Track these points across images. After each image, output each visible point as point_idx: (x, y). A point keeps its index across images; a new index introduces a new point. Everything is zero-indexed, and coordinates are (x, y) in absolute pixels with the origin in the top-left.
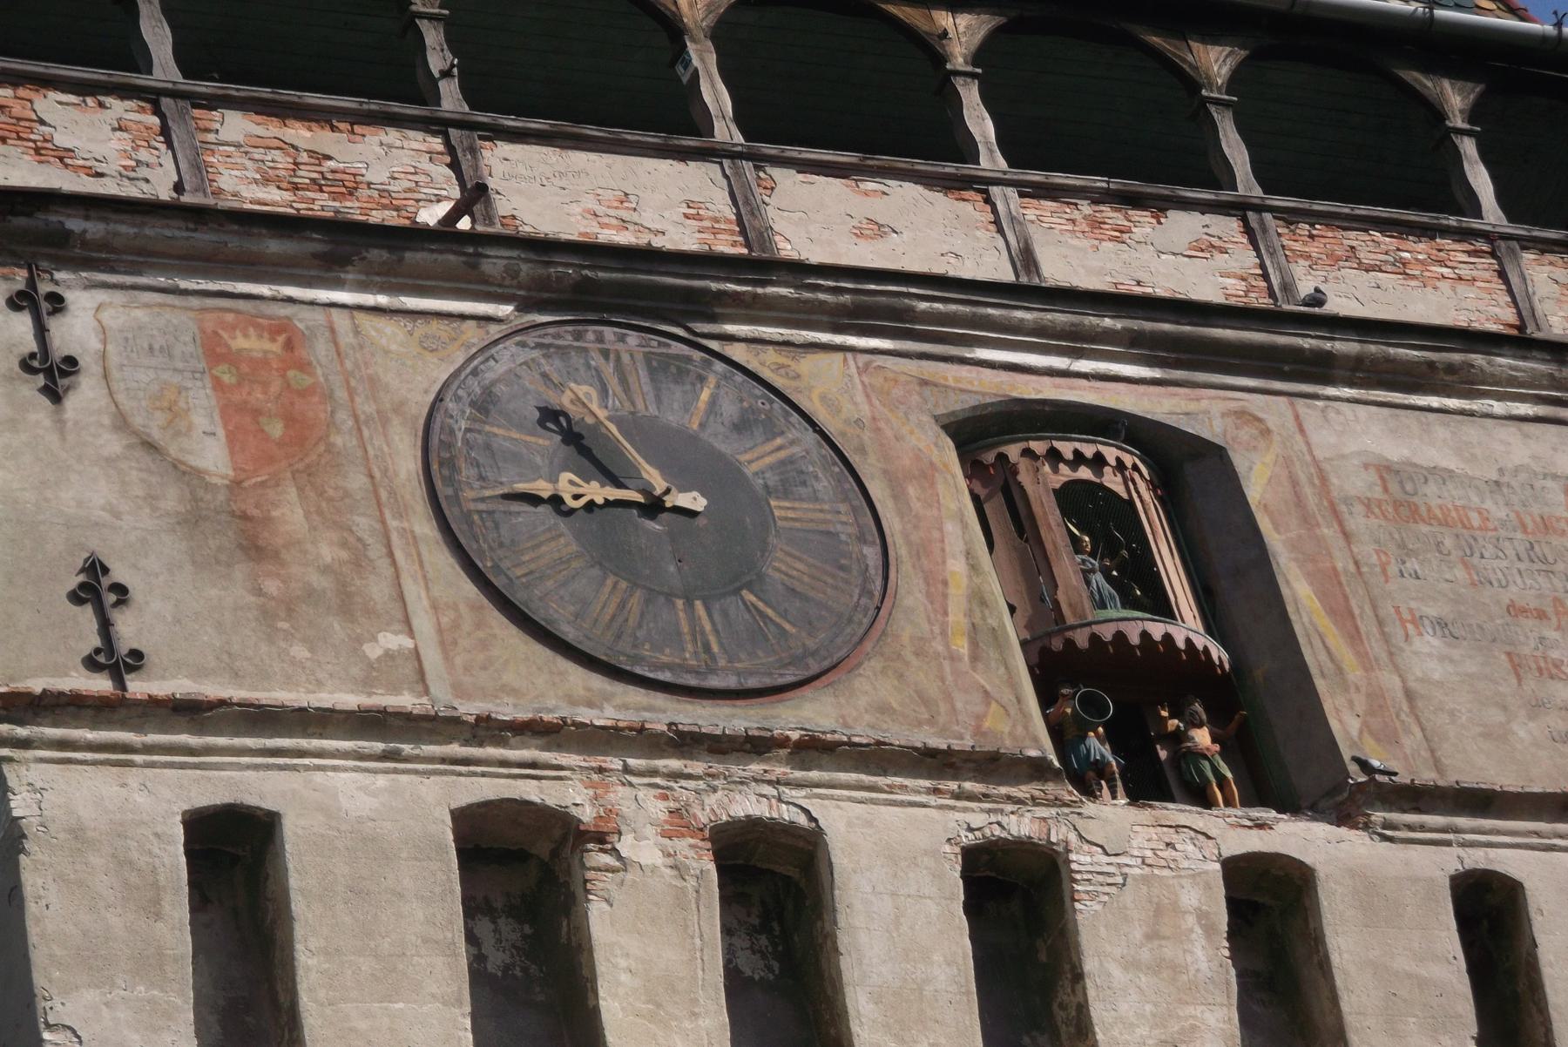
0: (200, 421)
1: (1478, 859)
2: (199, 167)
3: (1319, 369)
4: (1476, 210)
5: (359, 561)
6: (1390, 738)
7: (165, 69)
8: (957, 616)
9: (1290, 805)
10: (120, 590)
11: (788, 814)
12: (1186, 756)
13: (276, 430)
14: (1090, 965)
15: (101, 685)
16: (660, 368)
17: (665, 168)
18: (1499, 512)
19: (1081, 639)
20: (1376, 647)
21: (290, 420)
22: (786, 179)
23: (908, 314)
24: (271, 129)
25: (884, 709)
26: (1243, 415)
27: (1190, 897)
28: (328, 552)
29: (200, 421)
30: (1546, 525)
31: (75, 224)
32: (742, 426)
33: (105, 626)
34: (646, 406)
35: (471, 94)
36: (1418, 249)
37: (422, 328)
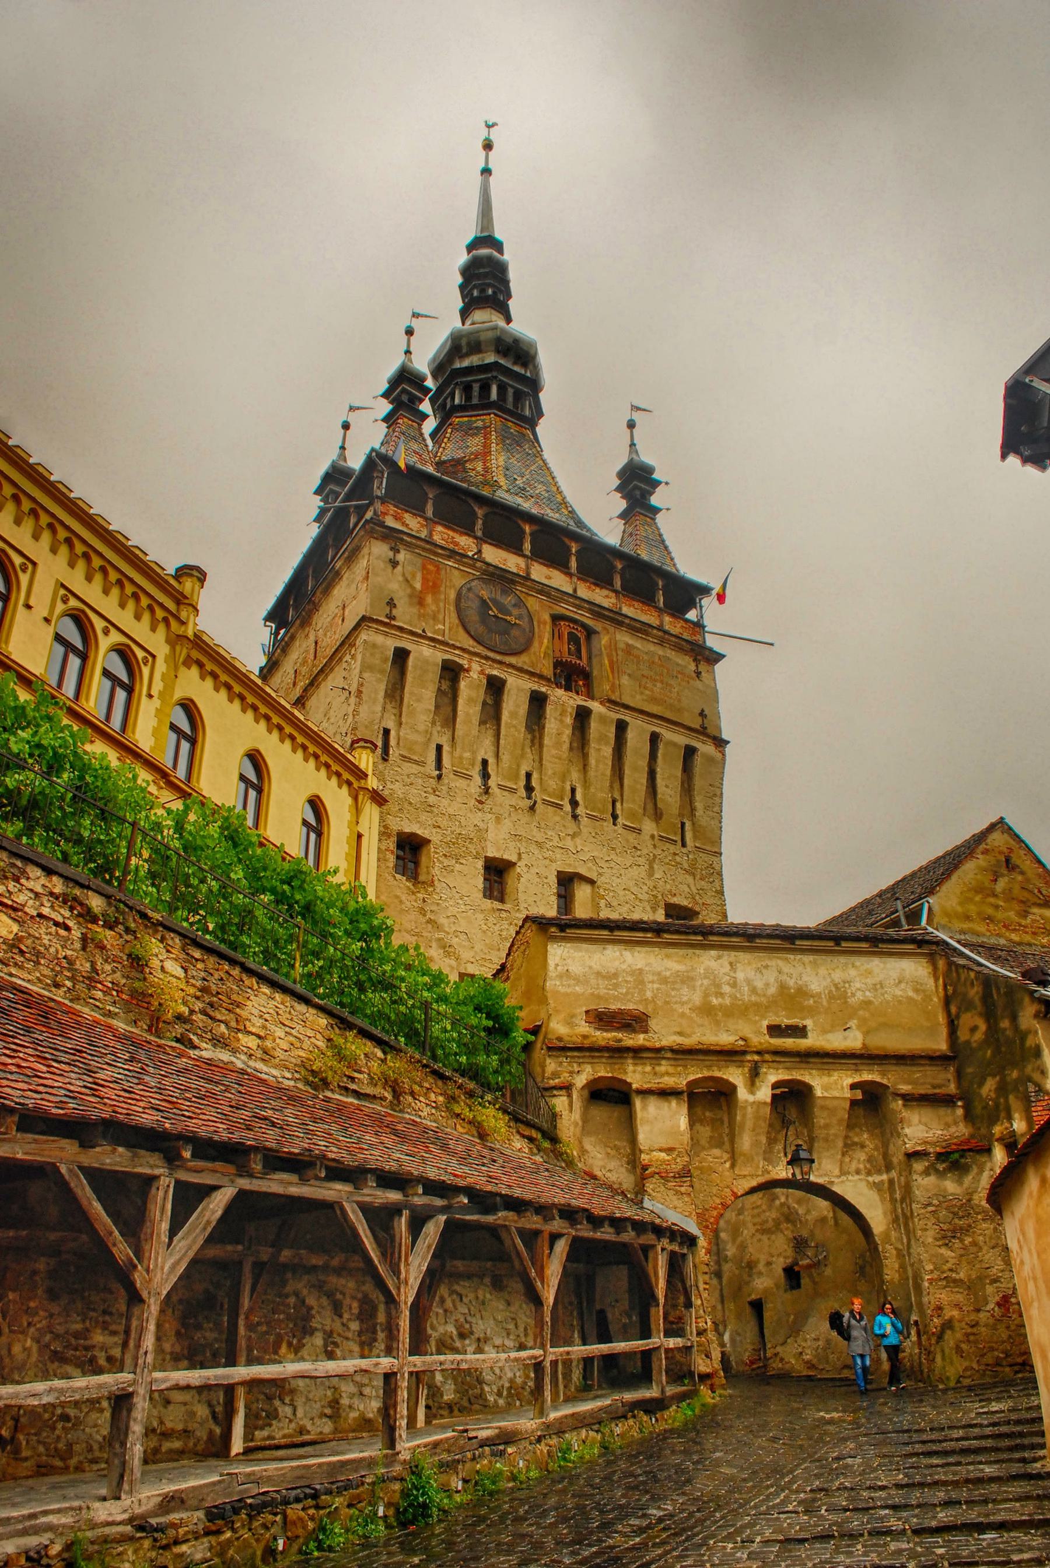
1: (622, 717)
2: (431, 535)
3: (620, 624)
5: (439, 611)
6: (613, 692)
7: (430, 513)
8: (543, 650)
9: (593, 698)
18: (646, 658)
22: (535, 564)
27: (569, 710)
28: (434, 608)
30: (653, 662)
32: (515, 605)
34: (498, 597)
35: (483, 533)
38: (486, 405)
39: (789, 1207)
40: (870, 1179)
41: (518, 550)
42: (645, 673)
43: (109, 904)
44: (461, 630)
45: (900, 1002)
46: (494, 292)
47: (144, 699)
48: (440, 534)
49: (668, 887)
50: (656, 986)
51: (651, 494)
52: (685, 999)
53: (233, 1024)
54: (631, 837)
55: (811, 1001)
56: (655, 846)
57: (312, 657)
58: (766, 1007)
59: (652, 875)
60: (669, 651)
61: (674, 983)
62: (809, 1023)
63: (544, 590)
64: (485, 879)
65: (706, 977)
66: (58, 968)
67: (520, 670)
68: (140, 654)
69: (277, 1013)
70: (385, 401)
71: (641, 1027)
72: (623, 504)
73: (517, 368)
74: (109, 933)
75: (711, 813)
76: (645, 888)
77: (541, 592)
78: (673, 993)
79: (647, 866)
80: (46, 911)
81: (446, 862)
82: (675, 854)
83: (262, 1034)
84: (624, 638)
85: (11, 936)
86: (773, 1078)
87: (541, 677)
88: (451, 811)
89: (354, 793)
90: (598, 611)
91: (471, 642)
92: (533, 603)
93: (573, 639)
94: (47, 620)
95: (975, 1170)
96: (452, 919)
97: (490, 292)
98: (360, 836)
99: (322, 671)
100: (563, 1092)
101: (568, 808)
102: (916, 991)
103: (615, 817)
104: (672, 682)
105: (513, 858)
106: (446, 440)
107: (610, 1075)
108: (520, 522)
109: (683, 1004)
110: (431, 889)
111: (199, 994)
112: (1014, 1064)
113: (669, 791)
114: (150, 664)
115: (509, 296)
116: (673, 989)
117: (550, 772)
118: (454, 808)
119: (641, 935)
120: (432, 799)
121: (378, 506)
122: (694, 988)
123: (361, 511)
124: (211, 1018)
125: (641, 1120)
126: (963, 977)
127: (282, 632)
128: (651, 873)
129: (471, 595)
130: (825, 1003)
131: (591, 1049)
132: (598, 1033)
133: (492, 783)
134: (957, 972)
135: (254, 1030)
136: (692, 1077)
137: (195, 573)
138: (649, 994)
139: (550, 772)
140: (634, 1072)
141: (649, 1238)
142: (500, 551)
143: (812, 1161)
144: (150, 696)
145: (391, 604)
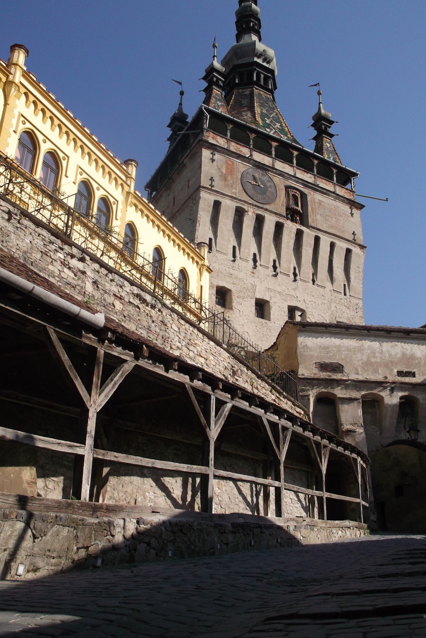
0: (224, 168)
1: (317, 234)
2: (229, 146)
3: (317, 190)
4: (334, 181)
5: (234, 183)
6: (313, 223)
7: (229, 137)
9: (304, 226)
10: (214, 180)
11: (263, 214)
12: (296, 219)
13: (230, 170)
14: (283, 234)
15: (210, 187)
16: (262, 174)
17: (268, 157)
18: (328, 206)
19: (291, 207)
20: (314, 214)
21: (231, 170)
22: (277, 161)
23: (284, 176)
24: (236, 145)
25: (273, 208)
26: (309, 192)
27: (293, 231)
29: (224, 168)
30: (331, 209)
31: (218, 148)
32: (268, 181)
33: (212, 183)
34: (261, 177)
36: (328, 183)
37: (244, 165)
38: (250, 83)
41: (269, 154)
42: (328, 214)
43: (152, 299)
44: (243, 191)
46: (253, 25)
47: (114, 220)
48: (234, 147)
49: (338, 314)
50: (346, 352)
51: (330, 127)
52: (360, 358)
53: (196, 352)
54: (321, 290)
55: (417, 361)
56: (332, 295)
57: (172, 204)
59: (331, 308)
60: (339, 203)
63: (282, 174)
64: (256, 308)
65: (369, 349)
66: (137, 324)
67: (271, 212)
68: (112, 200)
69: (211, 350)
70: (204, 81)
71: (340, 371)
72: (315, 133)
73: (265, 64)
74: (153, 311)
75: (358, 280)
76: (328, 314)
77: (279, 175)
78: (354, 356)
79: (328, 304)
80: (131, 300)
81: (239, 300)
82: (341, 299)
83: (206, 357)
84: (318, 196)
85: (121, 310)
86: (401, 394)
87: (280, 215)
88: (240, 277)
89: (199, 266)
90: (306, 184)
91: (249, 198)
92: (277, 179)
93: (295, 197)
94: (74, 183)
96: (241, 326)
97: (251, 25)
98: (201, 287)
99: (178, 211)
101: (292, 276)
103: (314, 281)
104: (340, 218)
105: (268, 299)
106: (232, 101)
108: (270, 141)
109: (358, 361)
110: (231, 312)
111: (184, 339)
113: (339, 270)
114: (116, 205)
115: (260, 27)
116: (354, 354)
117: (284, 260)
118: (241, 275)
120: (231, 271)
121: (206, 134)
122: (363, 354)
123: (196, 135)
124: (188, 349)
127: (154, 193)
128: (329, 308)
129: (248, 176)
131: (318, 379)
132: (321, 373)
133: (258, 264)
135: (203, 356)
136: (363, 393)
137: (133, 163)
138: (343, 356)
139: (284, 260)
141: (354, 456)
142: (261, 155)
143: (419, 431)
144: (117, 219)
145: (212, 179)
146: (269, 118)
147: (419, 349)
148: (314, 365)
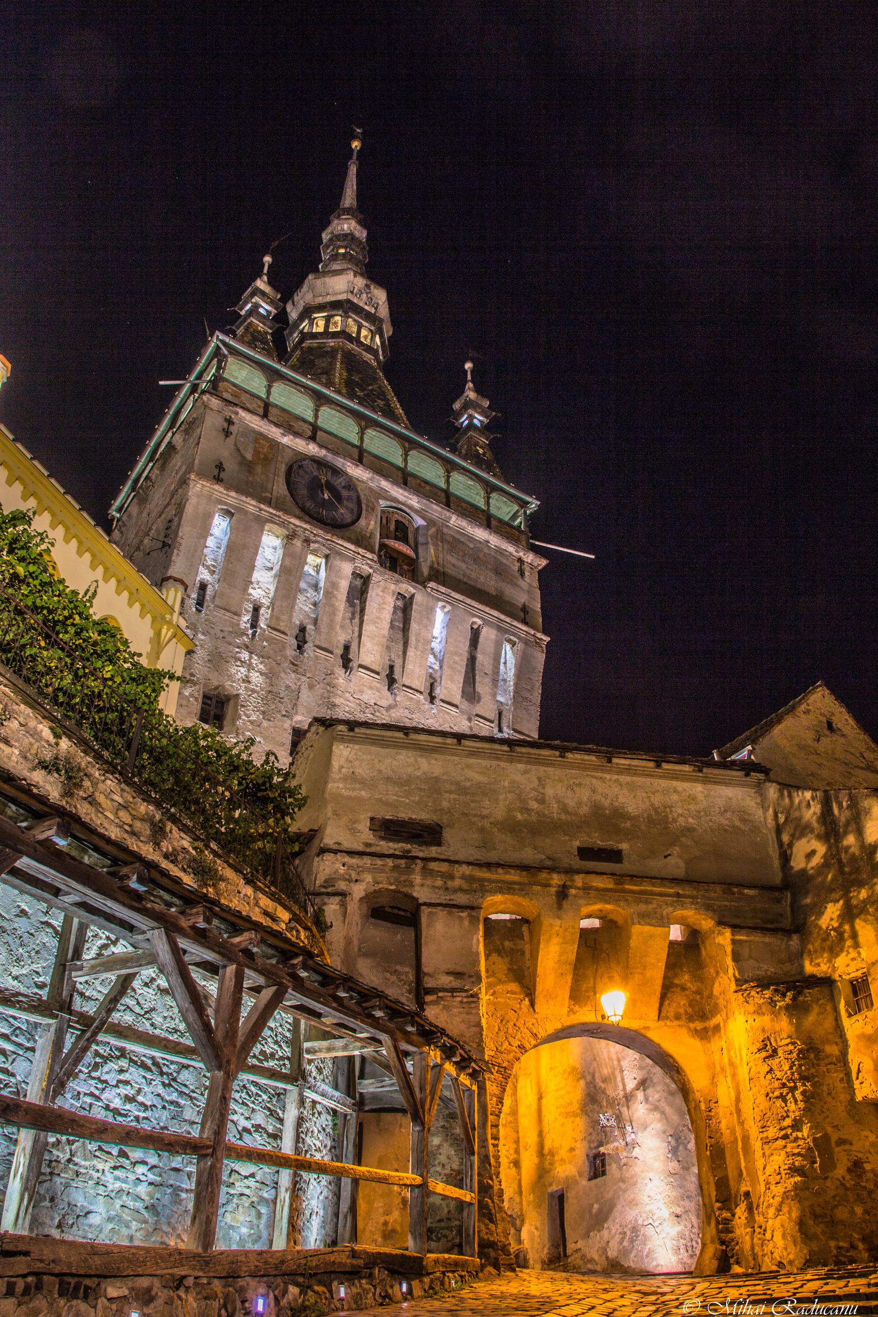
13: (262, 456)
31: (240, 411)
32: (344, 487)
39: (595, 1087)
40: (692, 1025)
45: (726, 830)
50: (452, 796)
52: (485, 812)
55: (628, 824)
58: (578, 827)
61: (473, 794)
62: (624, 846)
65: (510, 792)
78: (472, 805)
95: (816, 1009)
100: (337, 899)
102: (744, 821)
107: (393, 887)
109: (484, 817)
112: (861, 884)
116: (472, 802)
119: (440, 740)
125: (426, 937)
126: (797, 801)
129: (301, 472)
130: (643, 828)
132: (382, 843)
134: (790, 796)
138: (445, 804)
140: (422, 885)
145: (220, 467)
146: (362, 390)
147: (634, 797)
148: (368, 824)
